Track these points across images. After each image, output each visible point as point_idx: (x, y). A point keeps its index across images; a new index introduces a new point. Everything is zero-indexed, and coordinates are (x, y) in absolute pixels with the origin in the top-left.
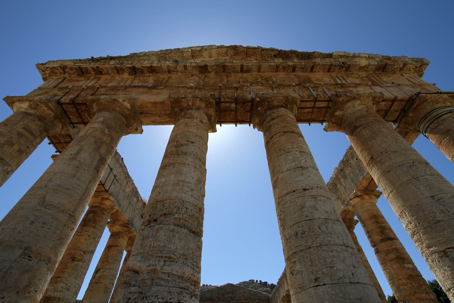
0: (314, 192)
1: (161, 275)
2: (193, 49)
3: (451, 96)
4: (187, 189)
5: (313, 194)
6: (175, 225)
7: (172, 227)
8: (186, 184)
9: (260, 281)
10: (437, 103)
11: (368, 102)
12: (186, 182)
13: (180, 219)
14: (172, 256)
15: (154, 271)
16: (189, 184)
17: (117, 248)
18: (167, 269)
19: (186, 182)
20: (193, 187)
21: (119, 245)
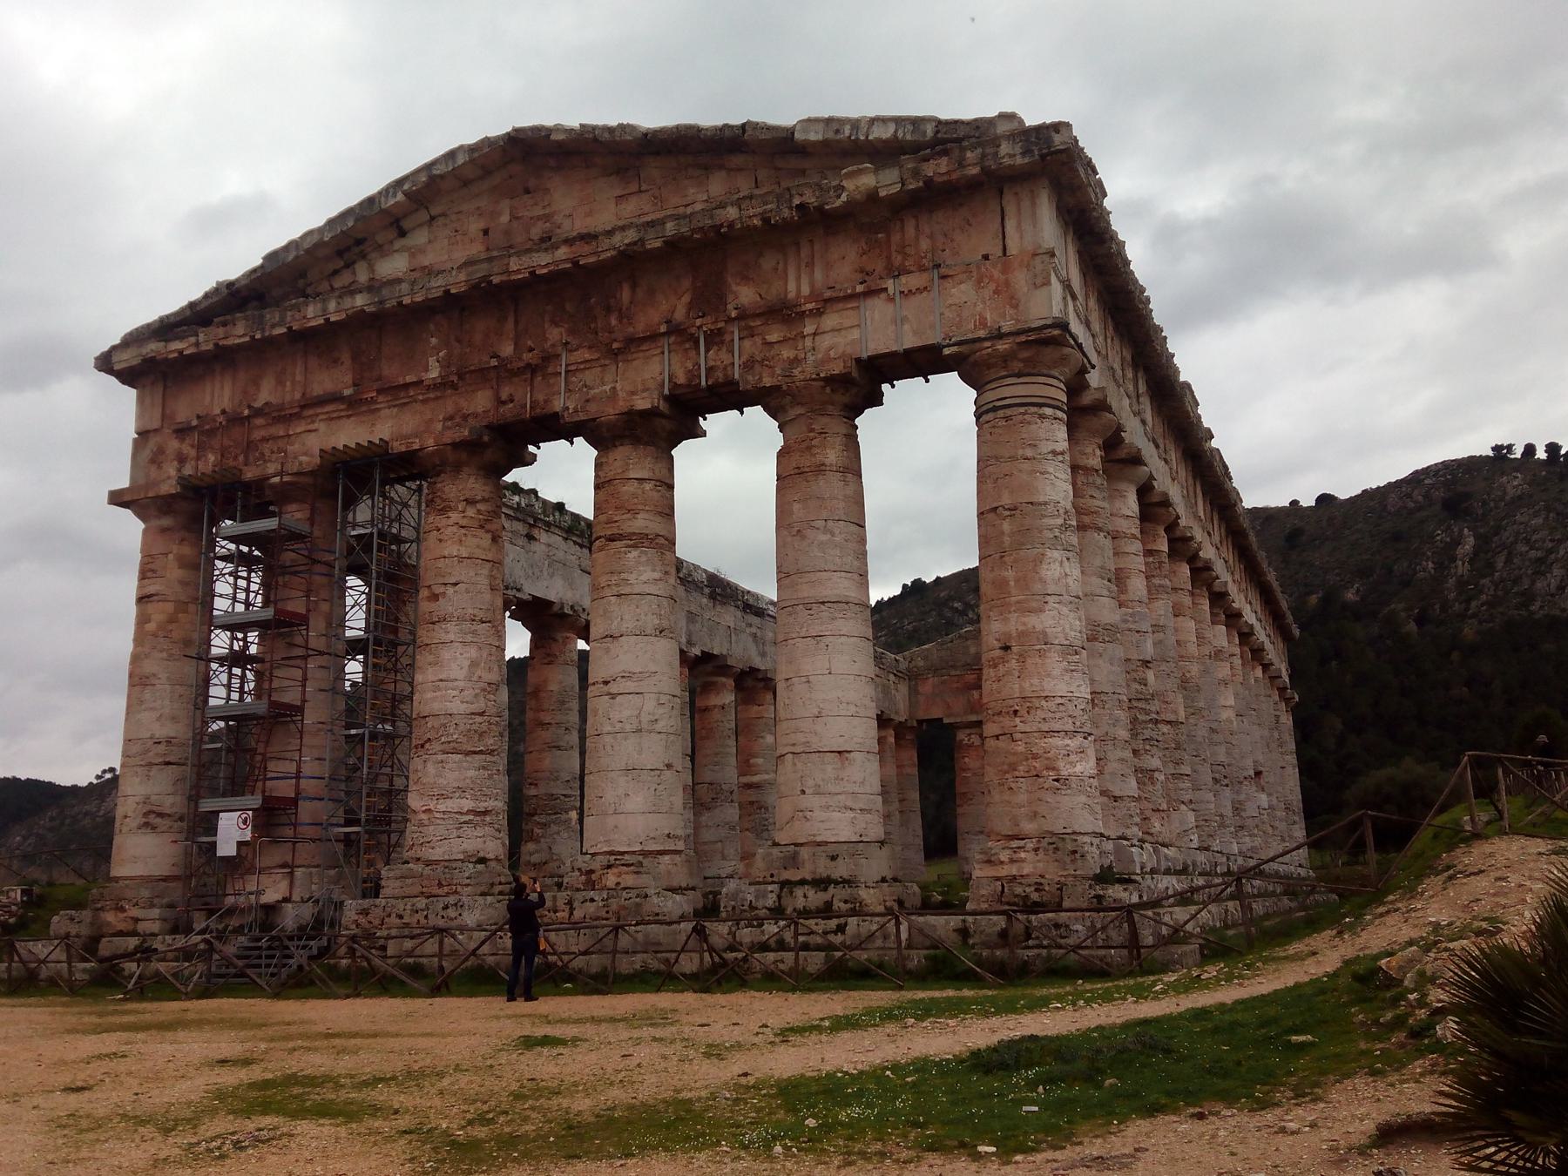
0: (613, 688)
1: (438, 815)
2: (406, 187)
4: (455, 693)
5: (612, 691)
6: (445, 752)
7: (440, 757)
8: (450, 684)
9: (1553, 448)
10: (989, 368)
12: (452, 681)
13: (449, 742)
14: (444, 792)
15: (429, 811)
16: (456, 683)
18: (442, 807)
19: (452, 681)
20: (461, 684)
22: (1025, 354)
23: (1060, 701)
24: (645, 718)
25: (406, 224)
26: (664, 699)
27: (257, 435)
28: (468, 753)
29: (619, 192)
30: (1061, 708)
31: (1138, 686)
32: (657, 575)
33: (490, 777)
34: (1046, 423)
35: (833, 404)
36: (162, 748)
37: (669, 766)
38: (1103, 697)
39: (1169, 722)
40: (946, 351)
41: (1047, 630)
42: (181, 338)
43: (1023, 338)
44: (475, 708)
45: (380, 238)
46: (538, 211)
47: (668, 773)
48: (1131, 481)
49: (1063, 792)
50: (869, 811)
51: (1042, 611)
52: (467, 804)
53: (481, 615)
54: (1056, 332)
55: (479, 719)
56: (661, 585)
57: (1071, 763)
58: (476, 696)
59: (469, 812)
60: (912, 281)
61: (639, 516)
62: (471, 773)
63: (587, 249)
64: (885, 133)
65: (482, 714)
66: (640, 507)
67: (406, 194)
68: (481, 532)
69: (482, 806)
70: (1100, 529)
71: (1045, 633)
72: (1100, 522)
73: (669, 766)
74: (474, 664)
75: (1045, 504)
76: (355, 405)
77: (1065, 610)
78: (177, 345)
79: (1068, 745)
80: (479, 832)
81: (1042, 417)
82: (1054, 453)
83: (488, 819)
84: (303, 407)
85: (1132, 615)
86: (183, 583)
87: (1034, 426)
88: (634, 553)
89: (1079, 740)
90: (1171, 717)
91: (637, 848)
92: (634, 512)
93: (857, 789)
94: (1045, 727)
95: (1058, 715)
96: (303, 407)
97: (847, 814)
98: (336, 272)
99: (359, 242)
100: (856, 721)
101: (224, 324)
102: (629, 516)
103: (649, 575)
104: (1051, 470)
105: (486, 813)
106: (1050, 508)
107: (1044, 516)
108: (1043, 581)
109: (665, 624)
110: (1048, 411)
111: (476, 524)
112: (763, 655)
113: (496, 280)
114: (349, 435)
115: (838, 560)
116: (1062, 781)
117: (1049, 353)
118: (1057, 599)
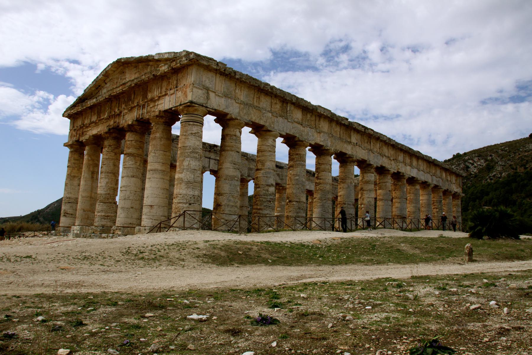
3: (185, 106)
20: (104, 187)
22: (186, 109)
24: (127, 196)
25: (106, 82)
26: (132, 192)
27: (84, 130)
28: (105, 203)
29: (135, 72)
31: (264, 192)
32: (133, 163)
33: (110, 208)
34: (190, 126)
36: (68, 199)
37: (132, 208)
38: (226, 194)
39: (297, 202)
40: (173, 109)
42: (73, 109)
43: (184, 105)
44: (106, 193)
45: (102, 85)
46: (124, 77)
47: (132, 209)
48: (270, 136)
50: (157, 220)
51: (182, 173)
52: (103, 214)
53: (110, 171)
54: (189, 104)
55: (107, 195)
56: (134, 165)
58: (107, 190)
59: (103, 216)
60: (172, 92)
62: (105, 207)
63: (123, 86)
64: (166, 56)
65: (109, 194)
67: (103, 75)
68: (111, 153)
69: (107, 215)
70: (233, 151)
71: (182, 178)
72: (233, 149)
73: (132, 208)
74: (107, 183)
75: (187, 146)
76: (96, 124)
77: (188, 173)
78: (72, 111)
80: (106, 220)
81: (189, 125)
82: (192, 134)
83: (109, 218)
84: (89, 124)
85: (266, 172)
86: (74, 163)
87: (187, 127)
88: (128, 158)
90: (298, 200)
91: (122, 226)
92: (129, 148)
93: (154, 214)
94: (179, 201)
96: (89, 124)
98: (97, 93)
99: (99, 86)
100: (156, 198)
101: (78, 106)
103: (131, 163)
104: (190, 138)
105: (108, 216)
106: (188, 148)
108: (183, 166)
109: (135, 174)
110: (191, 123)
111: (110, 150)
112: (282, 179)
113: (112, 94)
114: (94, 131)
117: (191, 109)
118: (186, 170)
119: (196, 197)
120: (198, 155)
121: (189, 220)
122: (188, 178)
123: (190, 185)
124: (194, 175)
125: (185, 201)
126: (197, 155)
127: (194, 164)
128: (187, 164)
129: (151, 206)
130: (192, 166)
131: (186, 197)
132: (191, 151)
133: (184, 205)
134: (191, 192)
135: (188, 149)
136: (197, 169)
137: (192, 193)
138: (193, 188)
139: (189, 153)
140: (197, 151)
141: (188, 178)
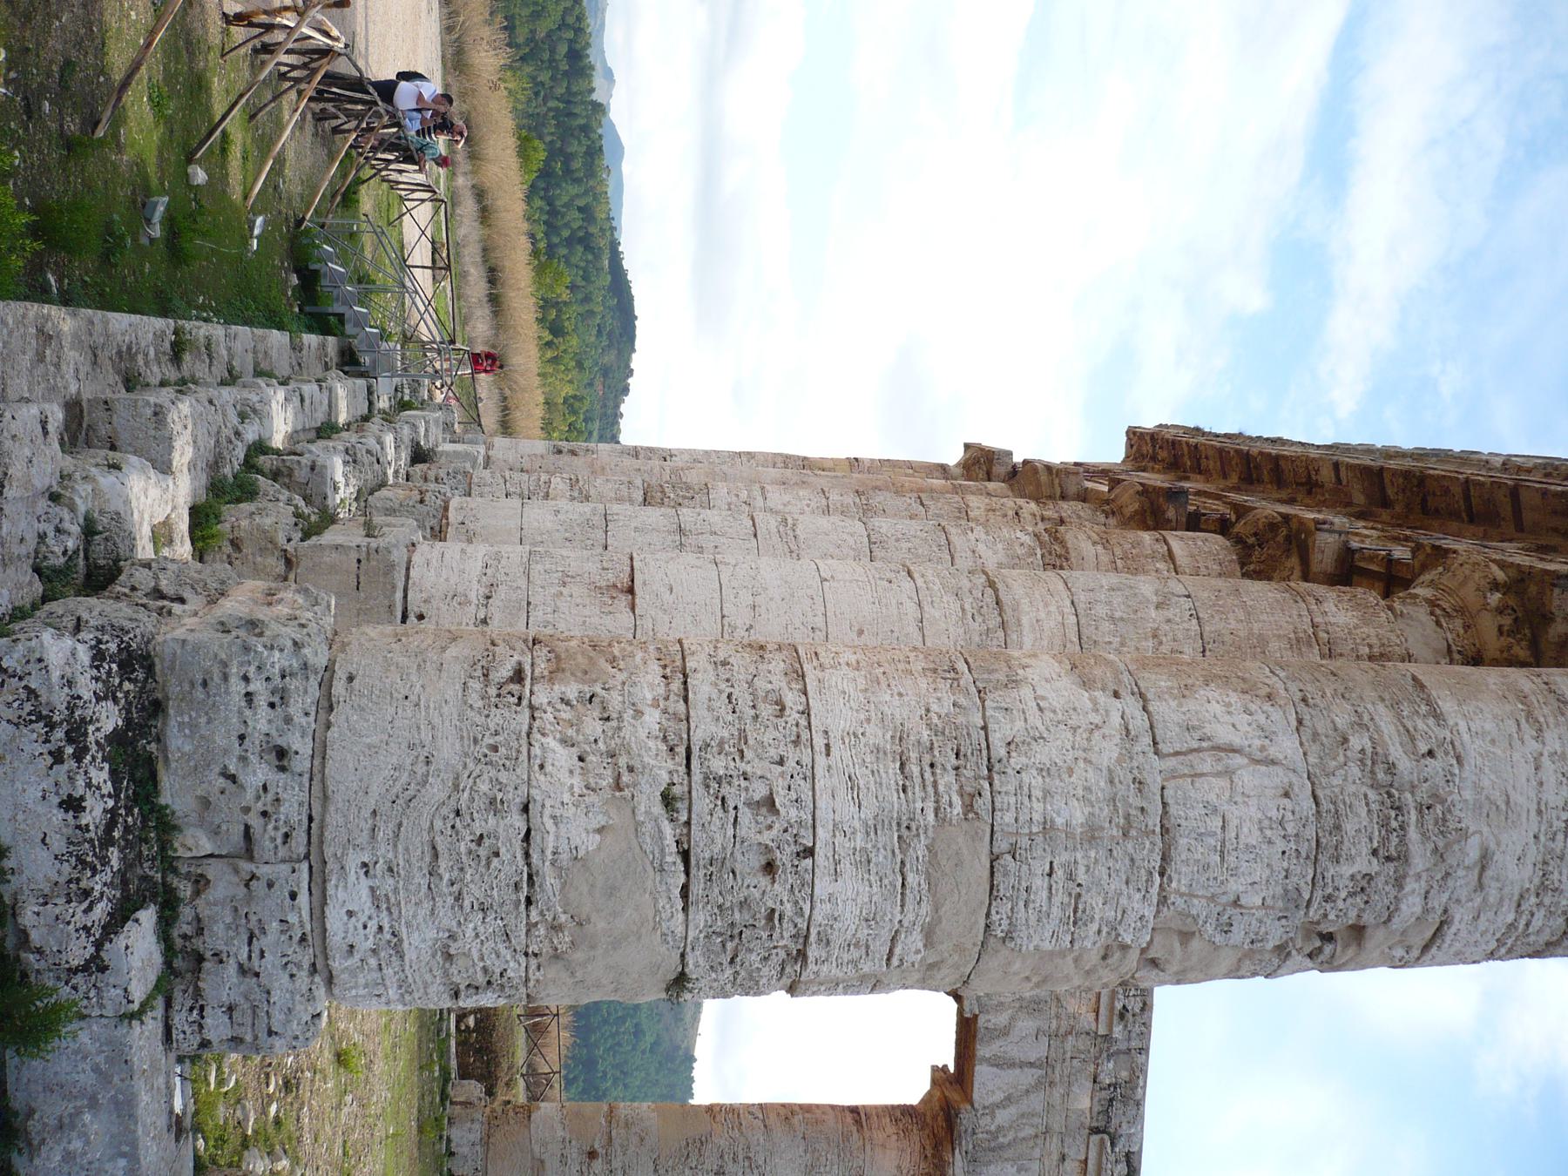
11: (1464, 583)
17: (854, 1129)
21: (867, 1134)
23: (792, 699)
30: (767, 710)
35: (1467, 627)
41: (1026, 692)
49: (476, 685)
57: (574, 724)
61: (1099, 547)
66: (1118, 551)
75: (1438, 716)
77: (1108, 751)
79: (639, 714)
89: (662, 769)
95: (744, 701)
97: (475, 586)
102: (1095, 537)
107: (1395, 706)
115: (1101, 610)
116: (514, 687)
119: (778, 893)
120: (1363, 886)
121: (436, 791)
122: (1043, 754)
123: (947, 780)
124: (1092, 835)
125: (703, 729)
126: (1363, 863)
127: (1246, 819)
128: (1224, 735)
129: (631, 591)
130: (1212, 790)
131: (770, 737)
132: (1404, 764)
133: (652, 718)
134: (847, 811)
135: (1410, 736)
136: (1179, 883)
137: (835, 806)
138: (906, 828)
139: (1358, 742)
140: (1420, 859)
141: (1043, 754)
